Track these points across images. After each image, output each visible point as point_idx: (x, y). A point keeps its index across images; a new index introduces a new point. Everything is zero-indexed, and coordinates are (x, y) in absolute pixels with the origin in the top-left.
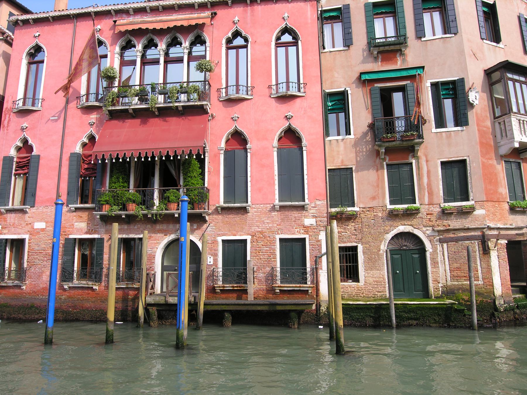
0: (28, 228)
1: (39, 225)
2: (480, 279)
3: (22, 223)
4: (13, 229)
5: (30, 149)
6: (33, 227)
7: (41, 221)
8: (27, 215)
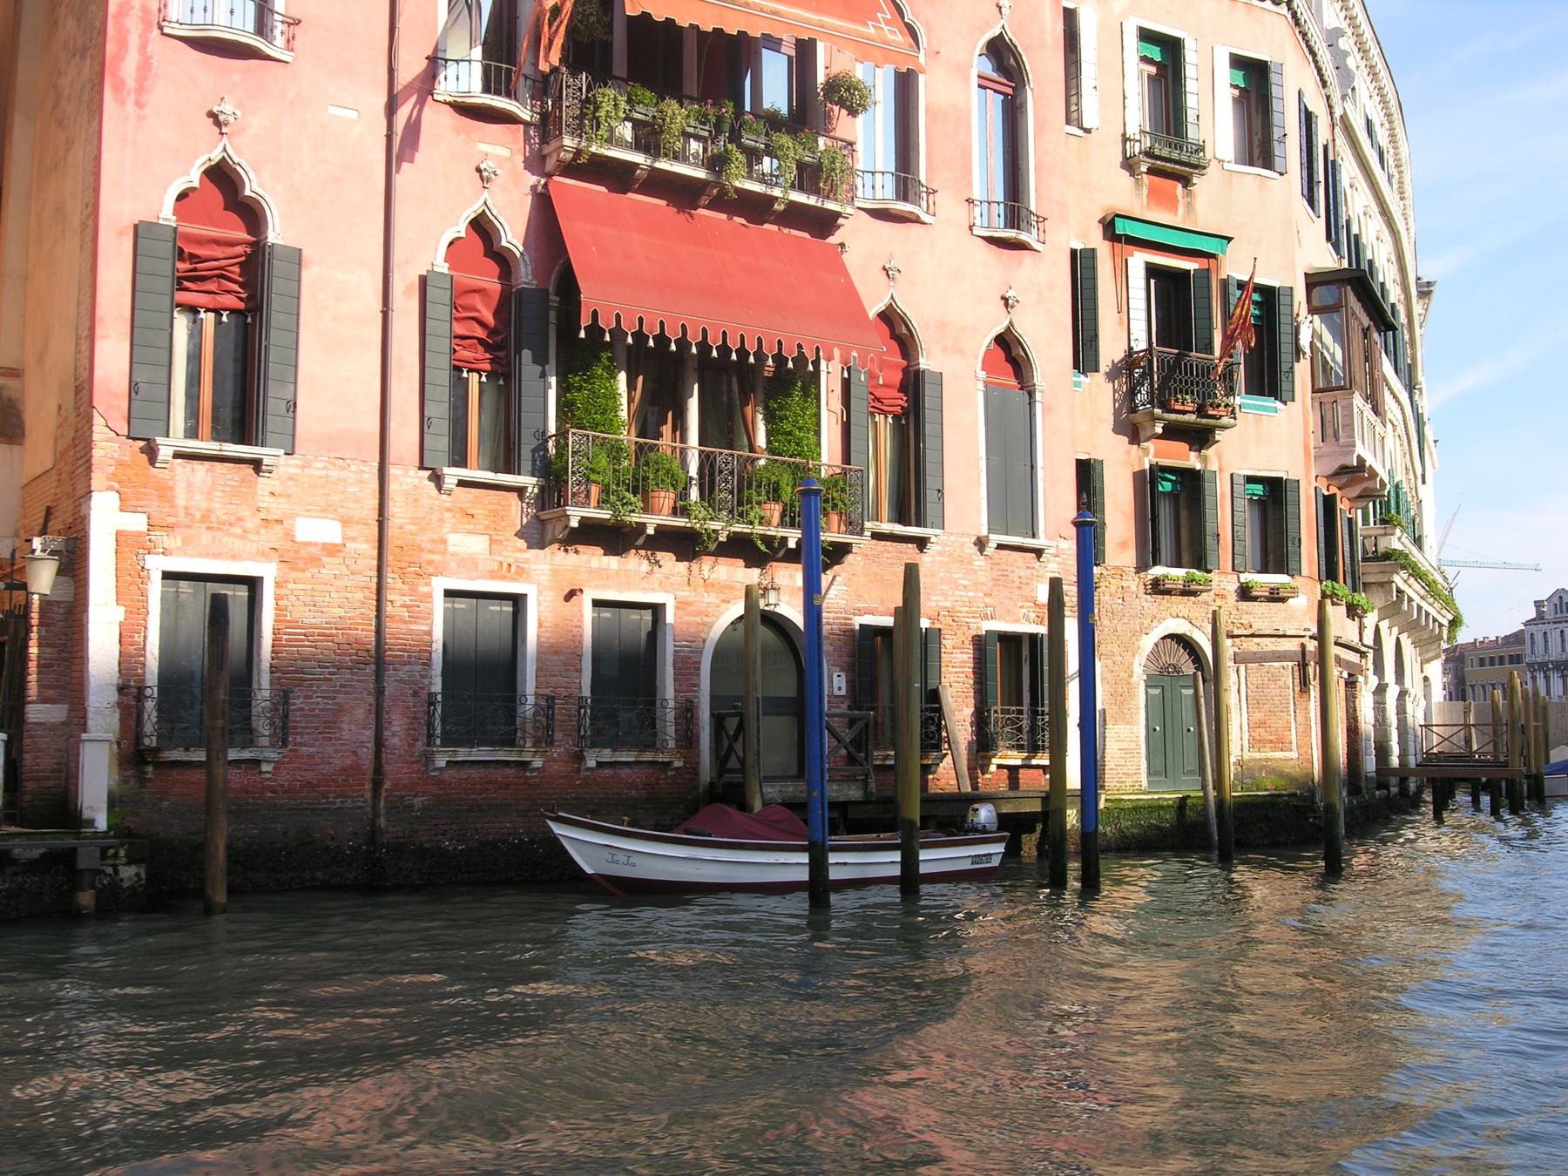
0: (271, 538)
1: (316, 530)
2: (1294, 746)
3: (245, 513)
4: (206, 538)
5: (251, 214)
6: (289, 536)
7: (325, 511)
8: (264, 483)
